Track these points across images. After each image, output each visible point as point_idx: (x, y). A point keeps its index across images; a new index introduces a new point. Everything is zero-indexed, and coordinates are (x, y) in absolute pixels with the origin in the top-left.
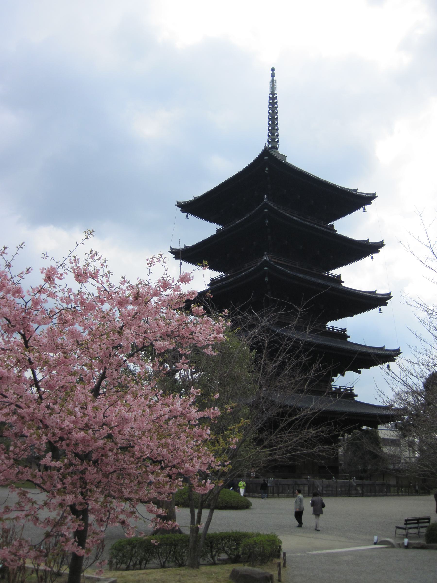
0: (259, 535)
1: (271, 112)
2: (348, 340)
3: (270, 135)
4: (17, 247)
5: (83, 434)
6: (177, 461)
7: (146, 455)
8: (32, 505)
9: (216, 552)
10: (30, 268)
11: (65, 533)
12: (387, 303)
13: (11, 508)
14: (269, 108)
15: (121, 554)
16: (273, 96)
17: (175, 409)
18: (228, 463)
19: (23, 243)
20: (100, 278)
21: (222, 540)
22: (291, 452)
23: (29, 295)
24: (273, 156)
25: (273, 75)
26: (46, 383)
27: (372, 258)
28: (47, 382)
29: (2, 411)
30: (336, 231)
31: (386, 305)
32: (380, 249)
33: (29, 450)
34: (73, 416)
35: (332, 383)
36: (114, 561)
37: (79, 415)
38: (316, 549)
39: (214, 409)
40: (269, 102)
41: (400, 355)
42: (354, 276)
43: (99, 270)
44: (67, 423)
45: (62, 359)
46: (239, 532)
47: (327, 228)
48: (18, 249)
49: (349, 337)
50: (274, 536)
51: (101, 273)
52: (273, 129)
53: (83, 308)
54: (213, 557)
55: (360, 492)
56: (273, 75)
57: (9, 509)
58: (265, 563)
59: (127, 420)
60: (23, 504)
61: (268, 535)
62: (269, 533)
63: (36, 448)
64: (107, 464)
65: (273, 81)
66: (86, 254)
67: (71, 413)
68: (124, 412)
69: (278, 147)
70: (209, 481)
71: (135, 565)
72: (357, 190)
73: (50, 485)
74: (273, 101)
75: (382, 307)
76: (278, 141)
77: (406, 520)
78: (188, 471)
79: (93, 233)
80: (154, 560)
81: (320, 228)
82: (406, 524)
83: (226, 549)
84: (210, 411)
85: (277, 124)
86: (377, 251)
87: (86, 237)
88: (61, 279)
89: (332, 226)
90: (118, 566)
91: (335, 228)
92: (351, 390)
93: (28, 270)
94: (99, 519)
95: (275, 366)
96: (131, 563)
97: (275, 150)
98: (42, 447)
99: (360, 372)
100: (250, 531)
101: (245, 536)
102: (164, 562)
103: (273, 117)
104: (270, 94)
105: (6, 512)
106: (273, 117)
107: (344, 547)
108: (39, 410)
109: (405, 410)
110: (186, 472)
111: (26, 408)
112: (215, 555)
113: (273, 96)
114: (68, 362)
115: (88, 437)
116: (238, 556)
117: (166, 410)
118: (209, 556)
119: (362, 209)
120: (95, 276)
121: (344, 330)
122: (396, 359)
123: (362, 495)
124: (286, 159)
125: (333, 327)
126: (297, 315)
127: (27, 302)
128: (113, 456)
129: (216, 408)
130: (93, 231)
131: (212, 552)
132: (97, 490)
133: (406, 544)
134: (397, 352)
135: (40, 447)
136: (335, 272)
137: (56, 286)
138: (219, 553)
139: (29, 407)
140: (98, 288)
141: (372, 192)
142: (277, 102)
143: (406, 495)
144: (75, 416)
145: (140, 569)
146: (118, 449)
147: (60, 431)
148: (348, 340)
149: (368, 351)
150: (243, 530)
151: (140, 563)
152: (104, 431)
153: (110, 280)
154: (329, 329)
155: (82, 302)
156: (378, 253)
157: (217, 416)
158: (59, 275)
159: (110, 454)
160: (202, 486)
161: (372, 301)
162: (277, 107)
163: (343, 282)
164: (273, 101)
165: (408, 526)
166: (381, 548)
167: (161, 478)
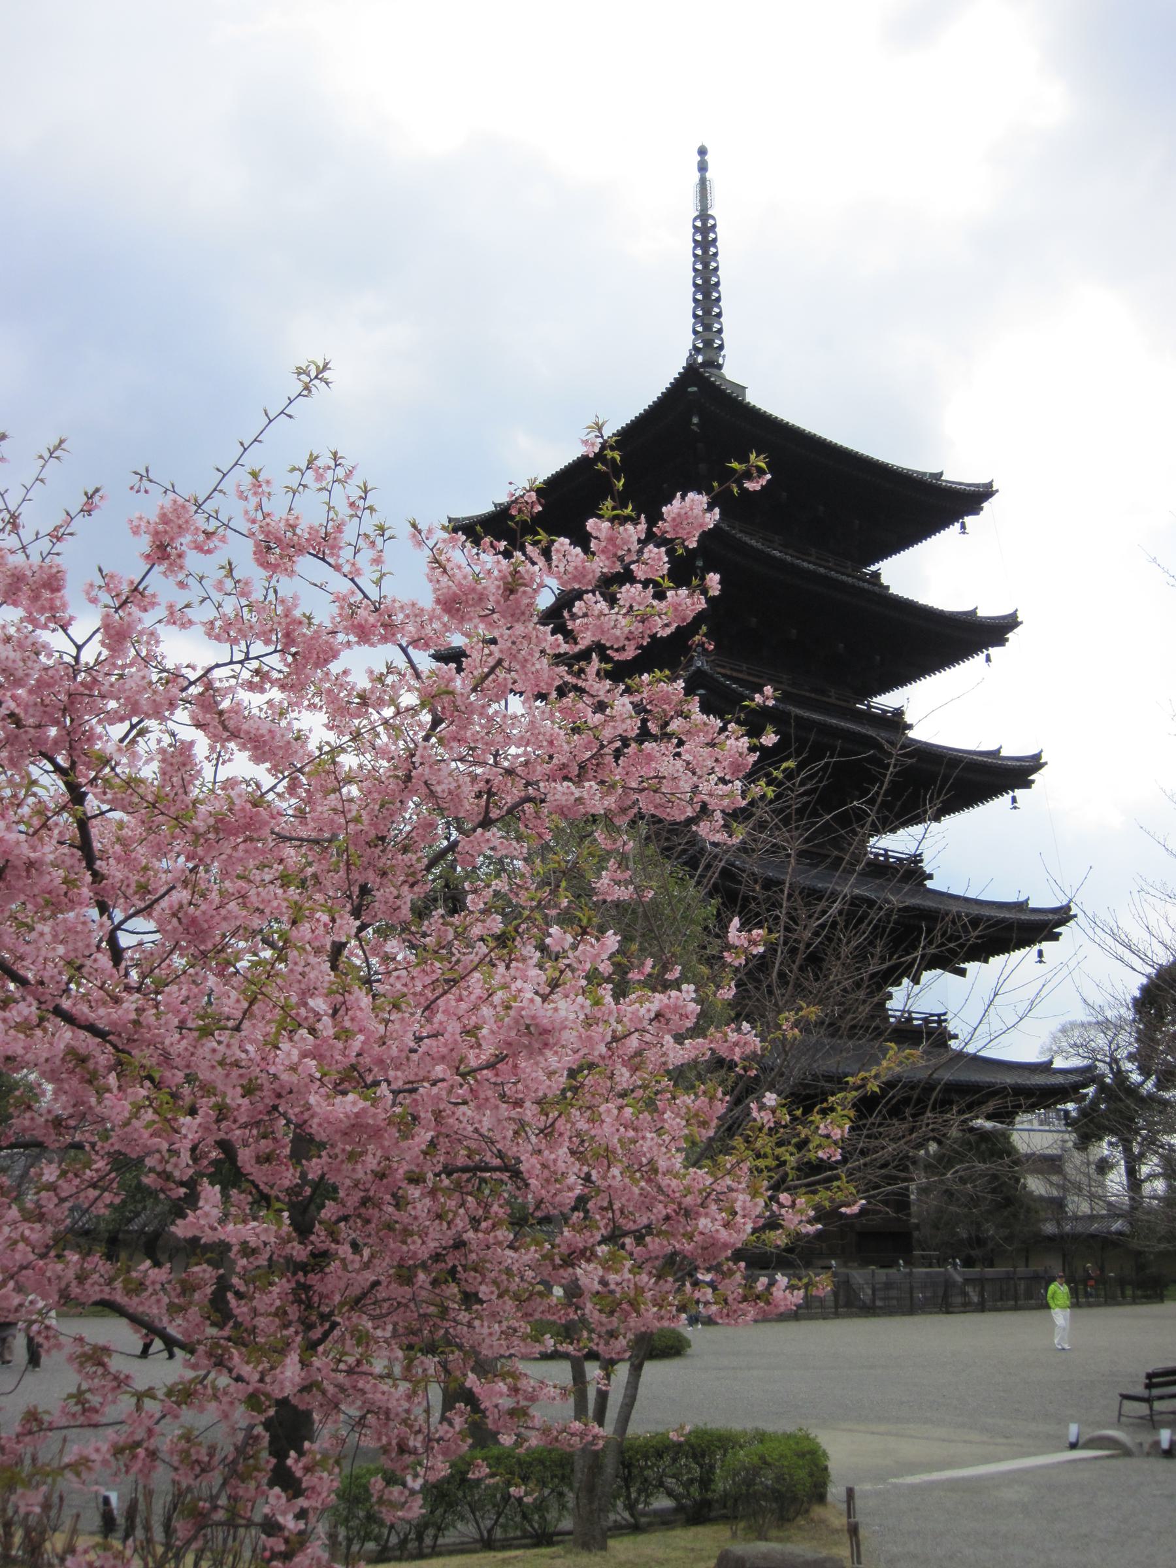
0: (761, 1437)
1: (699, 267)
2: (929, 884)
3: (700, 329)
4: (41, 457)
5: (354, 1103)
6: (660, 1210)
7: (570, 1189)
8: (139, 1407)
9: (639, 1491)
10: (97, 490)
11: (280, 1519)
12: (1033, 782)
13: (46, 1418)
14: (695, 255)
15: (361, 1514)
16: (704, 222)
17: (676, 1008)
18: (855, 1209)
19: (61, 442)
20: (347, 553)
21: (660, 1455)
22: (879, 1187)
23: (94, 601)
24: (713, 383)
25: (703, 168)
26: (174, 915)
27: (988, 659)
28: (181, 907)
29: (7, 1014)
30: (888, 587)
32: (1009, 636)
33: (115, 1185)
34: (303, 1032)
35: (889, 1004)
36: (342, 1532)
37: (326, 1027)
38: (913, 1467)
39: (739, 1030)
40: (695, 241)
41: (1071, 923)
42: (939, 710)
43: (343, 523)
44: (289, 1054)
45: (243, 809)
46: (705, 1432)
47: (859, 579)
48: (42, 462)
49: (930, 877)
50: (807, 1437)
51: (349, 534)
52: (707, 312)
53: (290, 659)
54: (631, 1507)
55: (976, 1299)
56: (703, 168)
57: (40, 1422)
58: (788, 1520)
59: (546, 1031)
60: (95, 1400)
61: (789, 1436)
62: (791, 1428)
63: (152, 1170)
64: (407, 1232)
65: (703, 183)
66: (293, 469)
67: (290, 1023)
68: (532, 1001)
70: (782, 1280)
71: (404, 1542)
72: (941, 474)
73: (198, 1319)
74: (705, 237)
75: (1018, 793)
76: (721, 347)
77: (1150, 1376)
78: (711, 1245)
79: (326, 375)
80: (459, 1525)
81: (844, 578)
82: (1149, 1386)
83: (670, 1482)
84: (726, 1034)
85: (718, 299)
86: (1000, 641)
87: (300, 386)
88: (209, 552)
89: (876, 575)
90: (355, 1548)
91: (885, 580)
92: (940, 1022)
93: (90, 498)
94: (394, 1442)
95: (822, 926)
96: (394, 1540)
97: (715, 371)
98: (176, 1165)
99: (962, 973)
100: (737, 1424)
101: (724, 1442)
102: (490, 1531)
103: (706, 281)
104: (695, 219)
105: (30, 1433)
106: (706, 281)
107: (987, 1460)
108: (158, 1016)
109: (1087, 1075)
110: (704, 1249)
111: (104, 1003)
112: (637, 1501)
113: (704, 222)
114: (266, 823)
115: (374, 1116)
116: (706, 1504)
117: (642, 1011)
118: (619, 1504)
119: (957, 525)
120: (323, 546)
121: (916, 859)
123: (981, 1308)
124: (744, 394)
125: (886, 850)
126: (887, 767)
127: (80, 643)
128: (427, 1201)
129: (746, 1026)
130: (326, 367)
131: (628, 1497)
132: (379, 1333)
133: (1165, 1445)
134: (1063, 915)
135: (169, 1168)
136: (887, 701)
137: (191, 581)
138: (648, 1496)
139: (117, 1001)
140: (338, 599)
141: (985, 480)
142: (715, 240)
143: (1099, 1305)
144: (312, 1031)
145: (420, 1555)
146: (436, 1175)
147: (246, 1101)
148: (929, 884)
149: (986, 912)
150: (717, 1422)
151: (420, 1538)
152: (435, 1090)
153: (386, 556)
154: (877, 855)
155: (287, 635)
157: (754, 1053)
158: (202, 537)
159: (414, 1192)
160: (758, 1297)
161: (987, 777)
162: (716, 254)
163: (910, 727)
164: (705, 237)
165: (1156, 1392)
166: (1096, 1458)
167: (622, 1278)
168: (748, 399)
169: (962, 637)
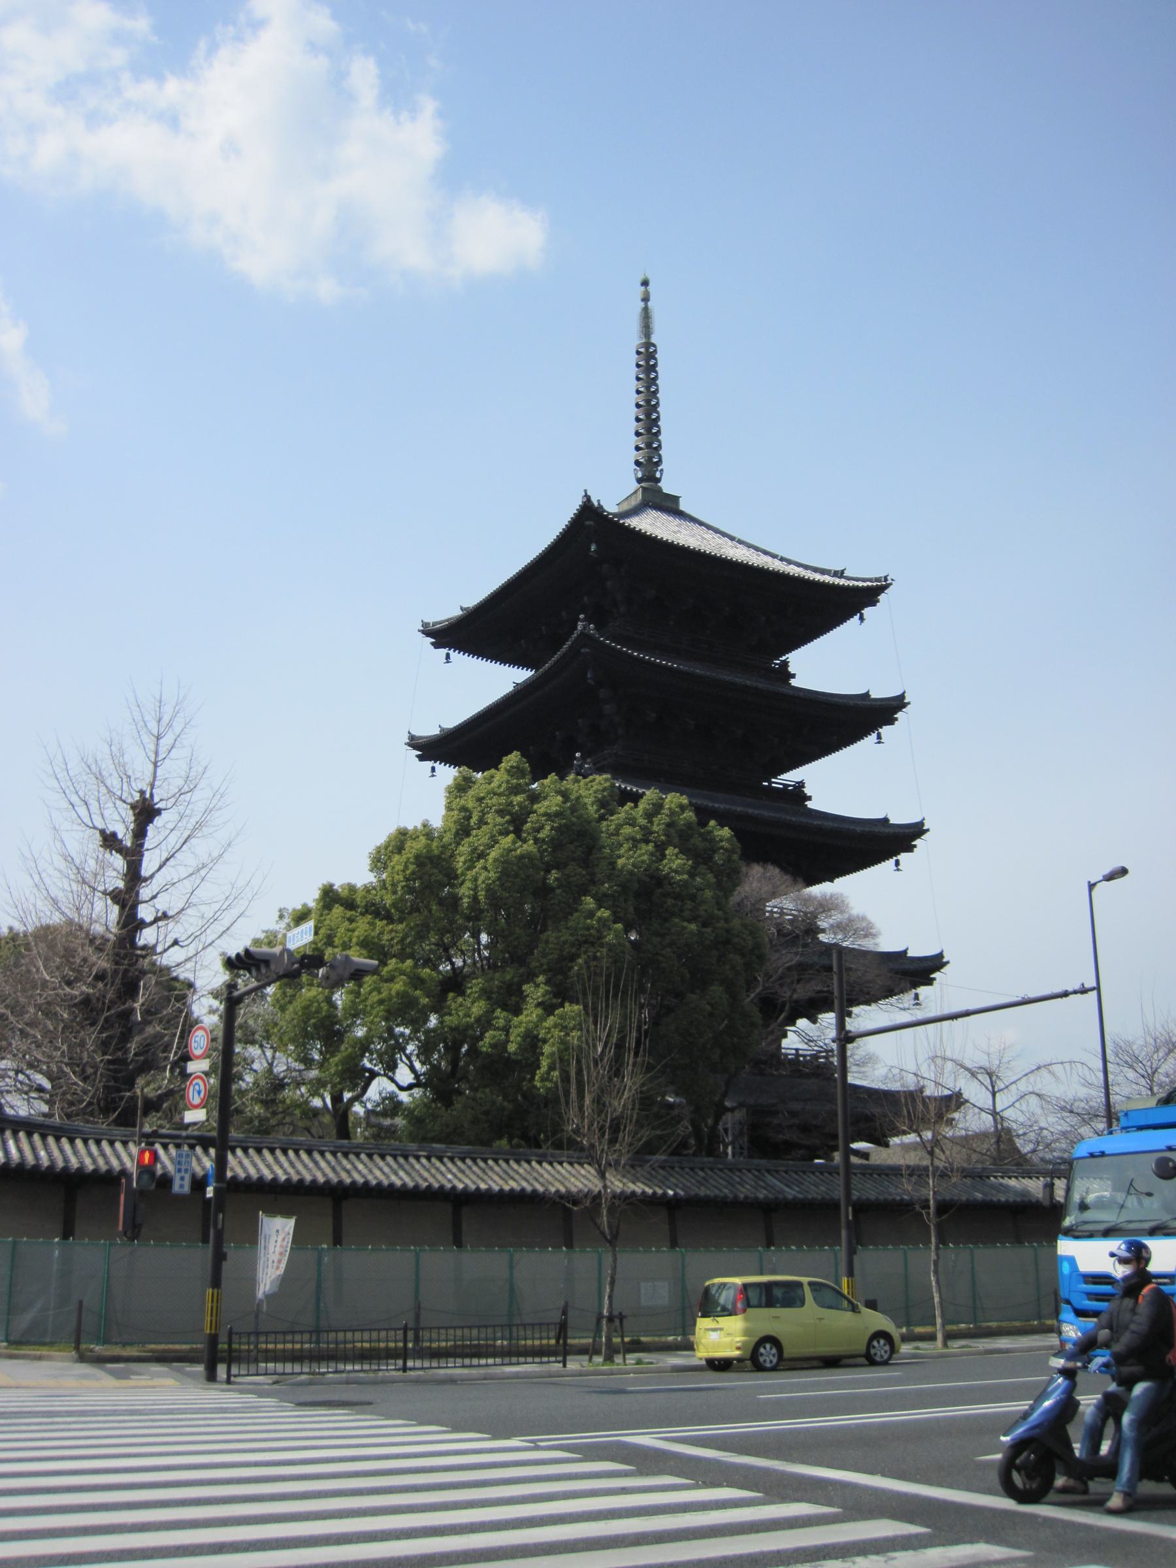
12: (915, 846)
31: (911, 851)
32: (899, 715)
42: (836, 784)
56: (646, 299)
69: (658, 475)
72: (843, 572)
86: (891, 721)
89: (785, 664)
91: (791, 669)
113: (647, 349)
119: (857, 617)
122: (934, 979)
136: (791, 777)
154: (771, 912)
156: (892, 724)
161: (882, 842)
163: (809, 798)
168: (682, 508)
169: (857, 719)
